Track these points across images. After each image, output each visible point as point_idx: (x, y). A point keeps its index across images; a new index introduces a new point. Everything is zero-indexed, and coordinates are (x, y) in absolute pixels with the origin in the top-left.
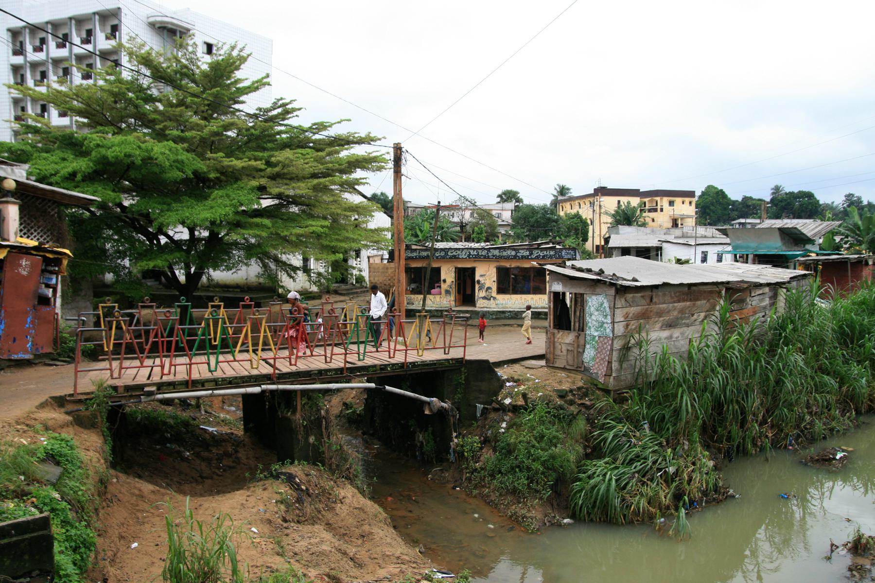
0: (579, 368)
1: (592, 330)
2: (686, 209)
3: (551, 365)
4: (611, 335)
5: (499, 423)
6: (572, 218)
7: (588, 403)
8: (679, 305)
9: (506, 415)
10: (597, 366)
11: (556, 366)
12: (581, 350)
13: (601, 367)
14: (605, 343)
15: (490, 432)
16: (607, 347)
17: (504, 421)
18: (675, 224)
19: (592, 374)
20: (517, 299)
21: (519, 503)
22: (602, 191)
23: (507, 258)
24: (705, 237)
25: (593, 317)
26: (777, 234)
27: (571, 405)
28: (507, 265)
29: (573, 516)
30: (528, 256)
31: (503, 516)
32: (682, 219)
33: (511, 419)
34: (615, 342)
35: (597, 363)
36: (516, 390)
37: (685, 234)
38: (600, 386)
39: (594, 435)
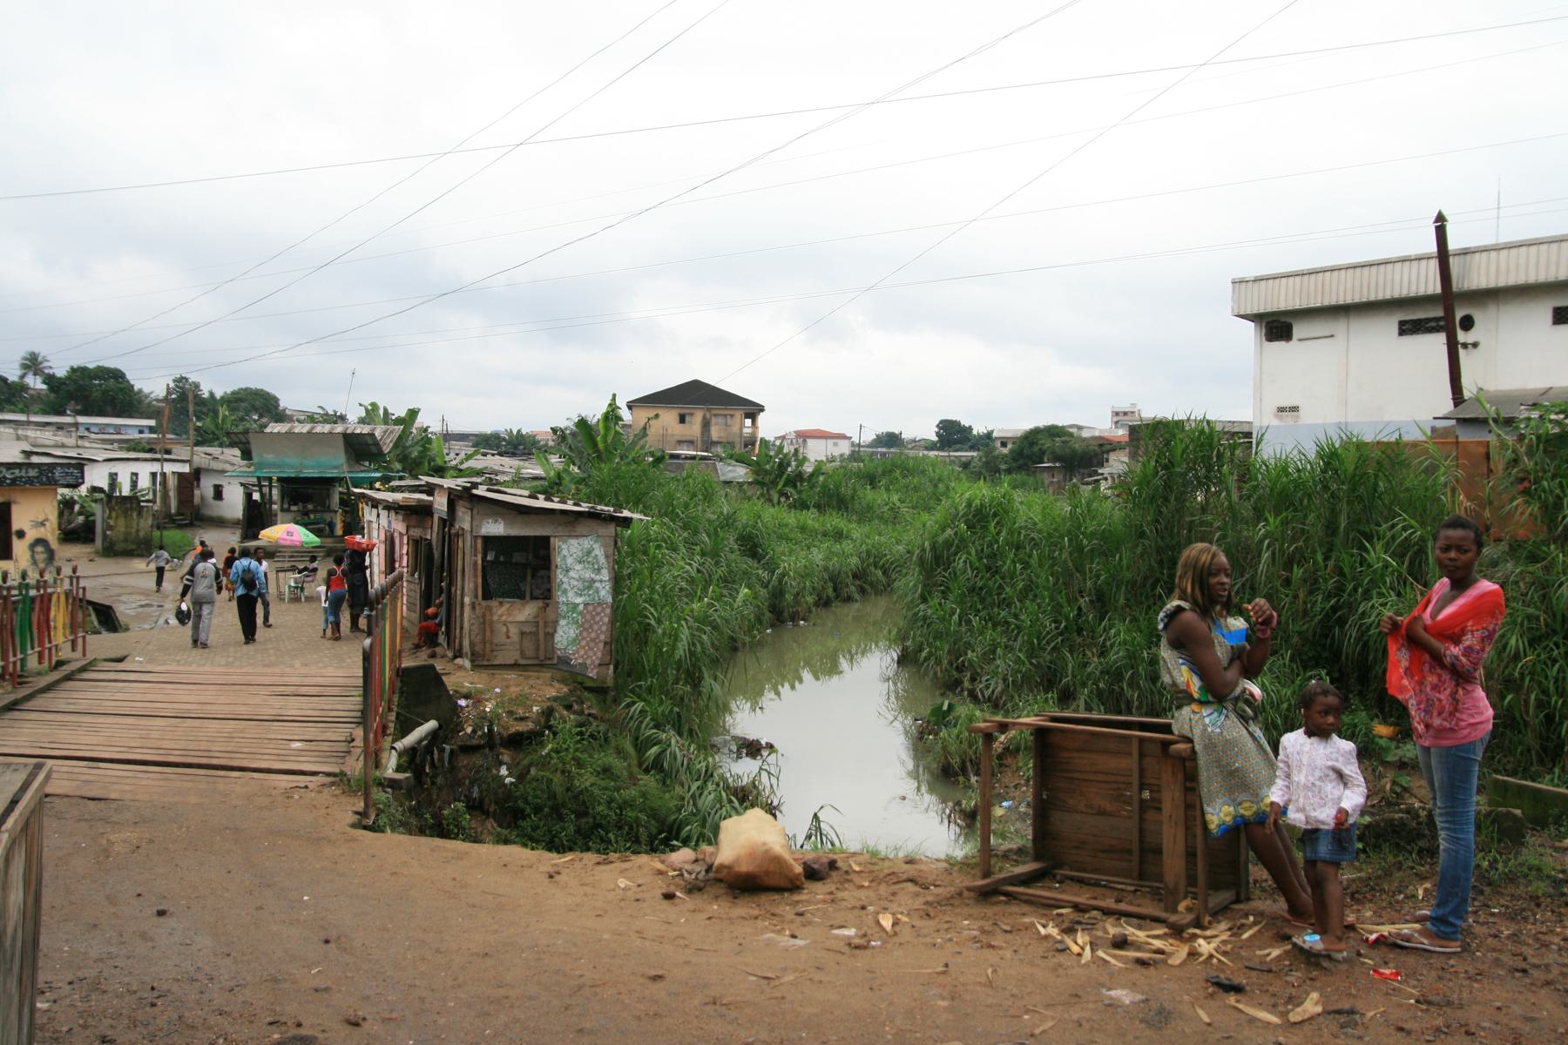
1: (570, 594)
10: (582, 652)
13: (591, 653)
14: (598, 614)
17: (501, 763)
25: (572, 574)
33: (513, 759)
35: (584, 648)
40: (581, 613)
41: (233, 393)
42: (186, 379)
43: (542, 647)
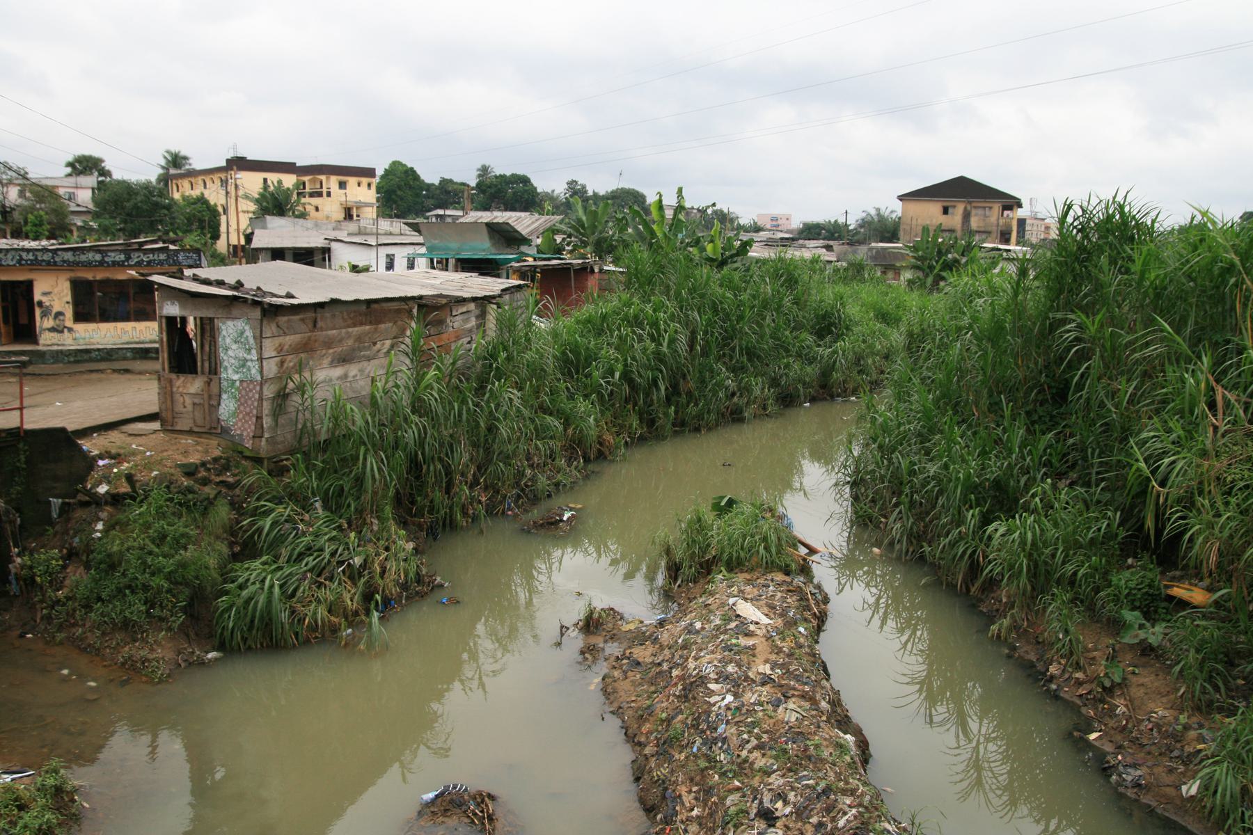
0: (215, 429)
1: (230, 371)
2: (363, 194)
3: (169, 428)
4: (259, 378)
5: (90, 524)
6: (193, 204)
7: (231, 480)
8: (355, 330)
9: (102, 511)
10: (240, 424)
11: (178, 428)
12: (214, 403)
13: (246, 426)
14: (251, 391)
15: (77, 540)
16: (253, 396)
17: (99, 519)
18: (348, 215)
19: (233, 436)
20: (108, 330)
21: (135, 640)
22: (239, 163)
23: (89, 265)
24: (391, 234)
25: (230, 353)
26: (485, 230)
27: (205, 485)
28: (89, 276)
29: (221, 647)
30: (123, 262)
31: (110, 666)
32: (358, 208)
33: (111, 515)
34: (265, 388)
35: (240, 420)
36: (115, 470)
37: (362, 229)
38: (247, 454)
39: (243, 526)
40: (238, 389)
41: (612, 192)
42: (576, 182)
43: (208, 418)
